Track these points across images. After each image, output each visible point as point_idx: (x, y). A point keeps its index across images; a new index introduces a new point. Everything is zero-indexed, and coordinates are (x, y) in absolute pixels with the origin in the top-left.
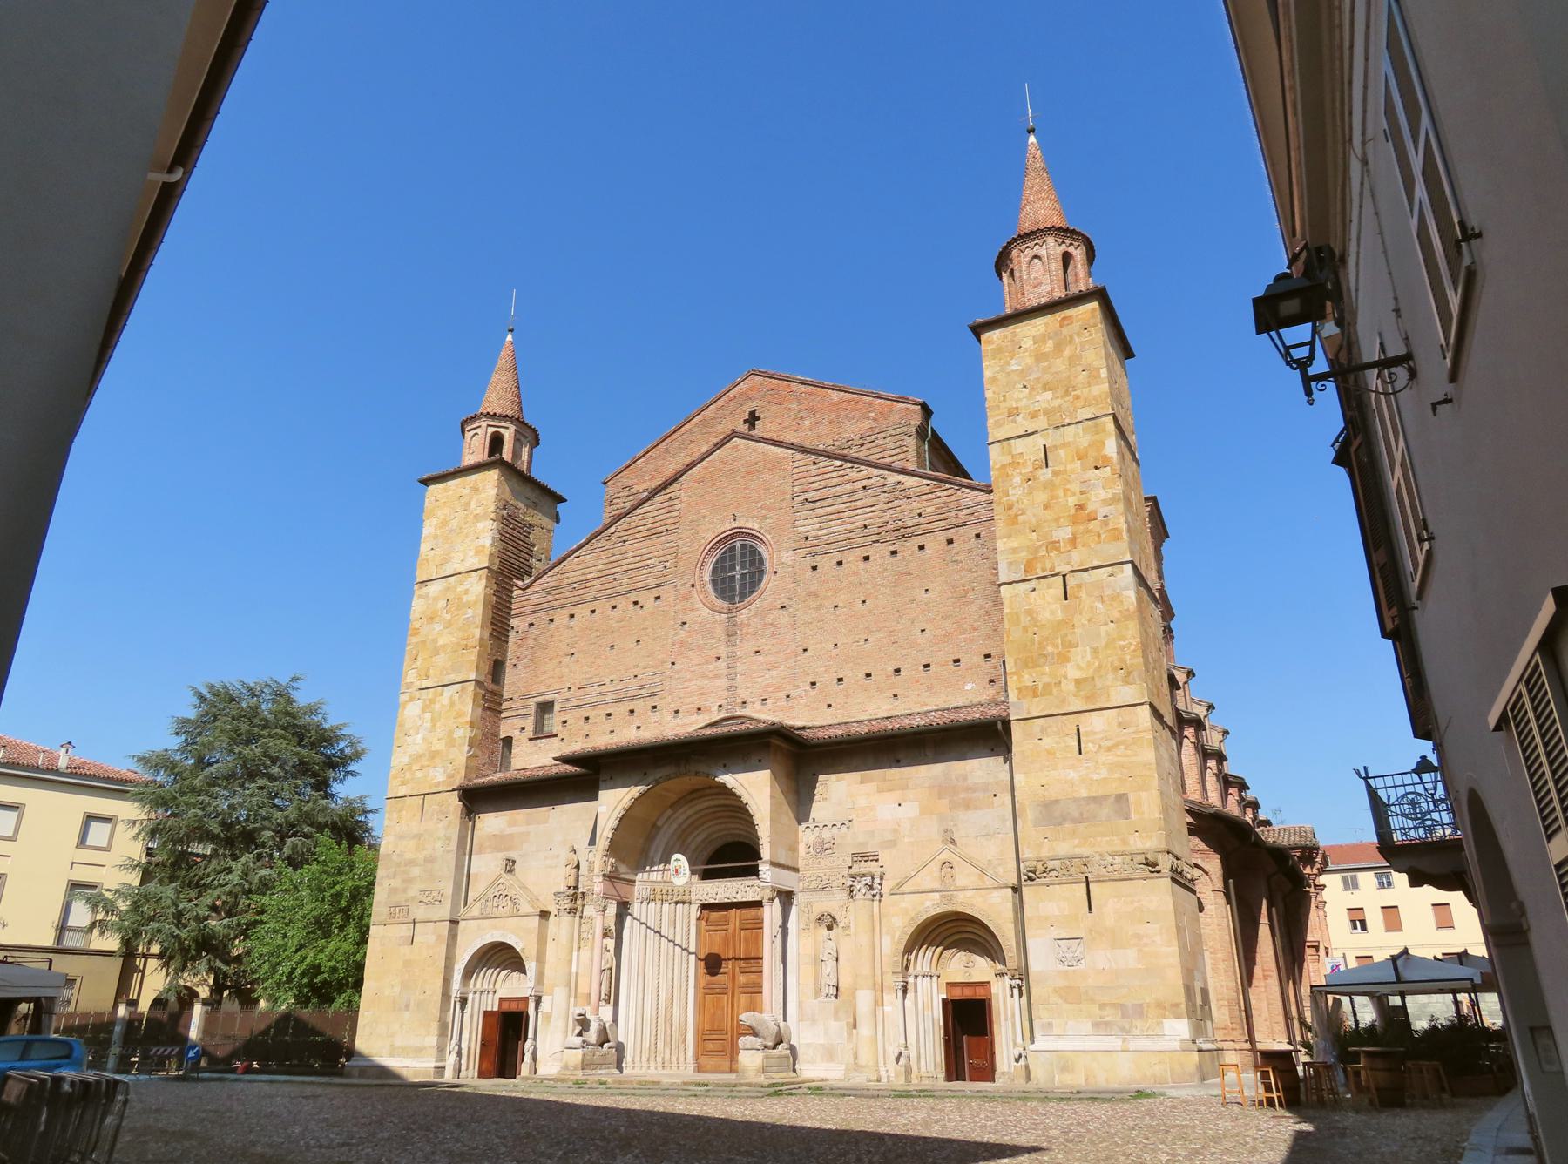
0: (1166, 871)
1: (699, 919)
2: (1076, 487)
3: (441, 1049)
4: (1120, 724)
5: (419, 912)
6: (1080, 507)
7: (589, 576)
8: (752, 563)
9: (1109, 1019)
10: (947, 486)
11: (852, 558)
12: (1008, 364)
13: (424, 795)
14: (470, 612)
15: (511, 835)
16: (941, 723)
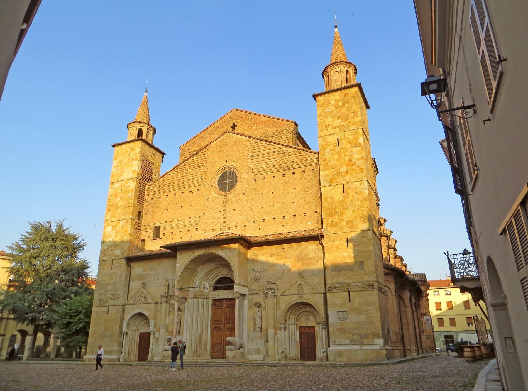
0: (376, 288)
2: (348, 153)
4: (361, 237)
5: (111, 302)
6: (350, 161)
7: (174, 182)
8: (233, 178)
9: (355, 339)
10: (303, 152)
11: (269, 177)
12: (326, 109)
14: (130, 194)
16: (299, 236)
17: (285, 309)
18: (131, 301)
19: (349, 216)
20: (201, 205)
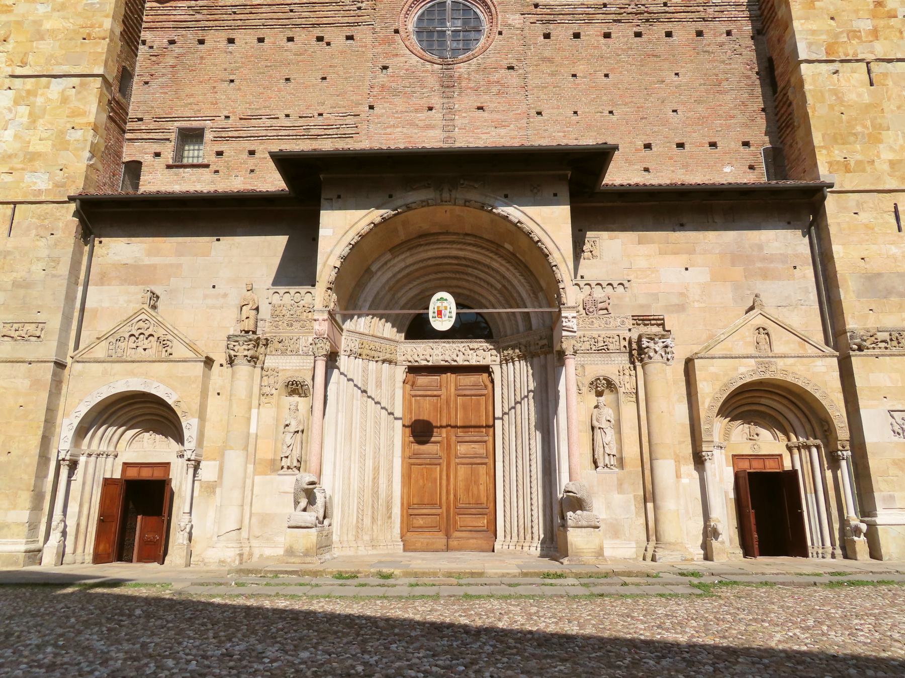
3: (33, 527)
11: (592, 33)
13: (15, 203)
15: (154, 267)
17: (716, 399)
18: (100, 351)
19: (897, 148)
20: (359, 81)
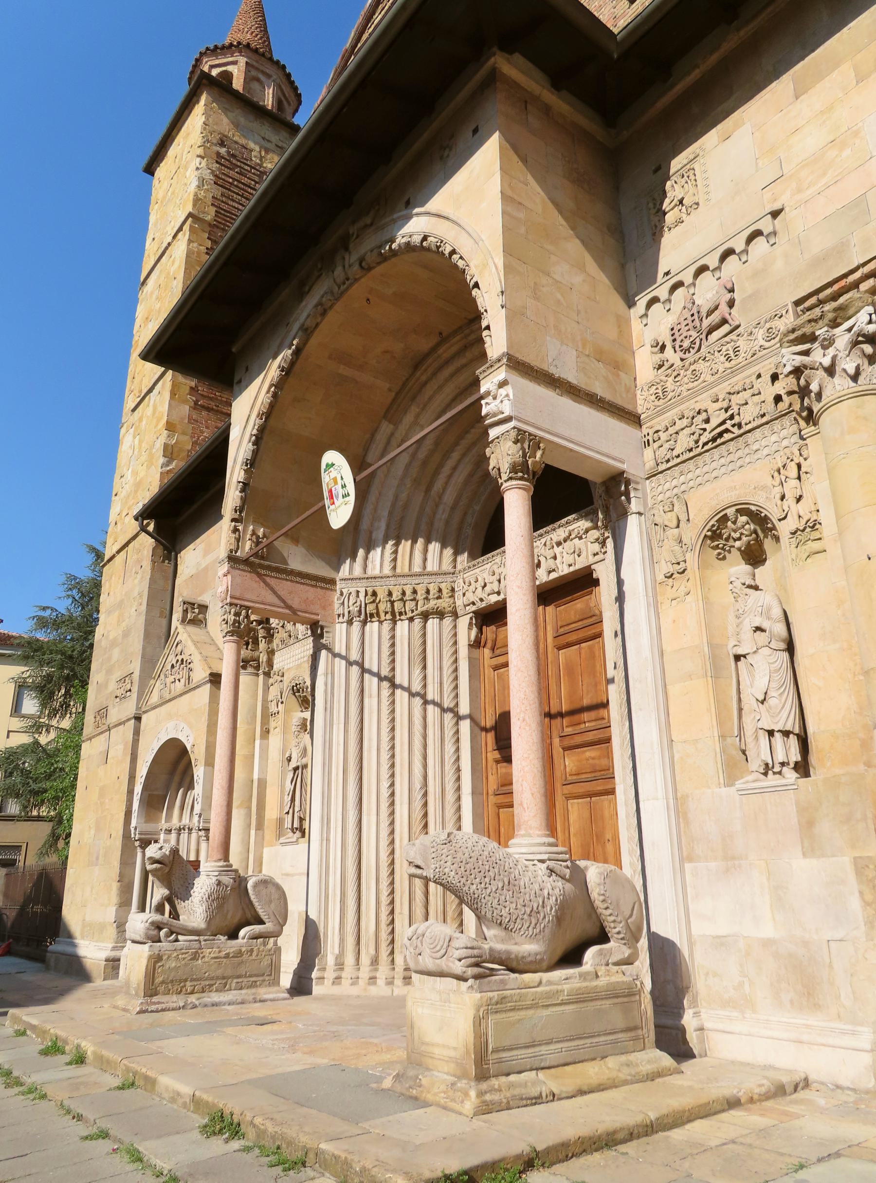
1: (476, 644)
